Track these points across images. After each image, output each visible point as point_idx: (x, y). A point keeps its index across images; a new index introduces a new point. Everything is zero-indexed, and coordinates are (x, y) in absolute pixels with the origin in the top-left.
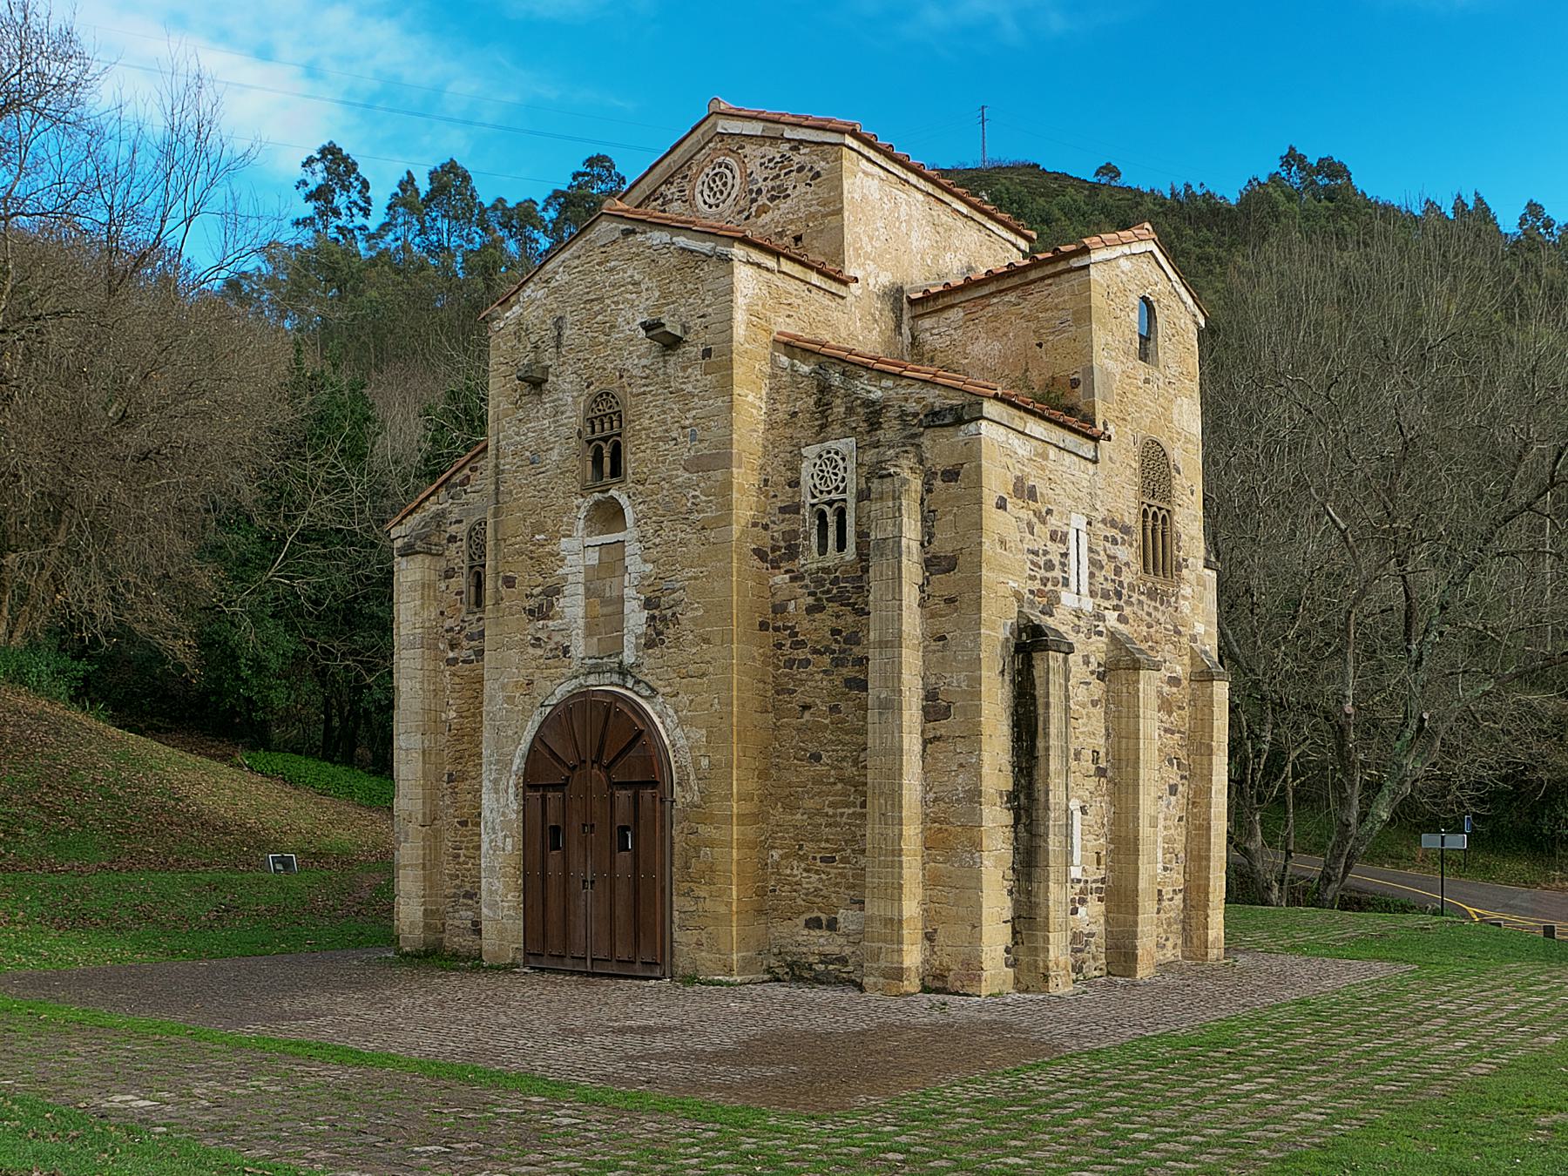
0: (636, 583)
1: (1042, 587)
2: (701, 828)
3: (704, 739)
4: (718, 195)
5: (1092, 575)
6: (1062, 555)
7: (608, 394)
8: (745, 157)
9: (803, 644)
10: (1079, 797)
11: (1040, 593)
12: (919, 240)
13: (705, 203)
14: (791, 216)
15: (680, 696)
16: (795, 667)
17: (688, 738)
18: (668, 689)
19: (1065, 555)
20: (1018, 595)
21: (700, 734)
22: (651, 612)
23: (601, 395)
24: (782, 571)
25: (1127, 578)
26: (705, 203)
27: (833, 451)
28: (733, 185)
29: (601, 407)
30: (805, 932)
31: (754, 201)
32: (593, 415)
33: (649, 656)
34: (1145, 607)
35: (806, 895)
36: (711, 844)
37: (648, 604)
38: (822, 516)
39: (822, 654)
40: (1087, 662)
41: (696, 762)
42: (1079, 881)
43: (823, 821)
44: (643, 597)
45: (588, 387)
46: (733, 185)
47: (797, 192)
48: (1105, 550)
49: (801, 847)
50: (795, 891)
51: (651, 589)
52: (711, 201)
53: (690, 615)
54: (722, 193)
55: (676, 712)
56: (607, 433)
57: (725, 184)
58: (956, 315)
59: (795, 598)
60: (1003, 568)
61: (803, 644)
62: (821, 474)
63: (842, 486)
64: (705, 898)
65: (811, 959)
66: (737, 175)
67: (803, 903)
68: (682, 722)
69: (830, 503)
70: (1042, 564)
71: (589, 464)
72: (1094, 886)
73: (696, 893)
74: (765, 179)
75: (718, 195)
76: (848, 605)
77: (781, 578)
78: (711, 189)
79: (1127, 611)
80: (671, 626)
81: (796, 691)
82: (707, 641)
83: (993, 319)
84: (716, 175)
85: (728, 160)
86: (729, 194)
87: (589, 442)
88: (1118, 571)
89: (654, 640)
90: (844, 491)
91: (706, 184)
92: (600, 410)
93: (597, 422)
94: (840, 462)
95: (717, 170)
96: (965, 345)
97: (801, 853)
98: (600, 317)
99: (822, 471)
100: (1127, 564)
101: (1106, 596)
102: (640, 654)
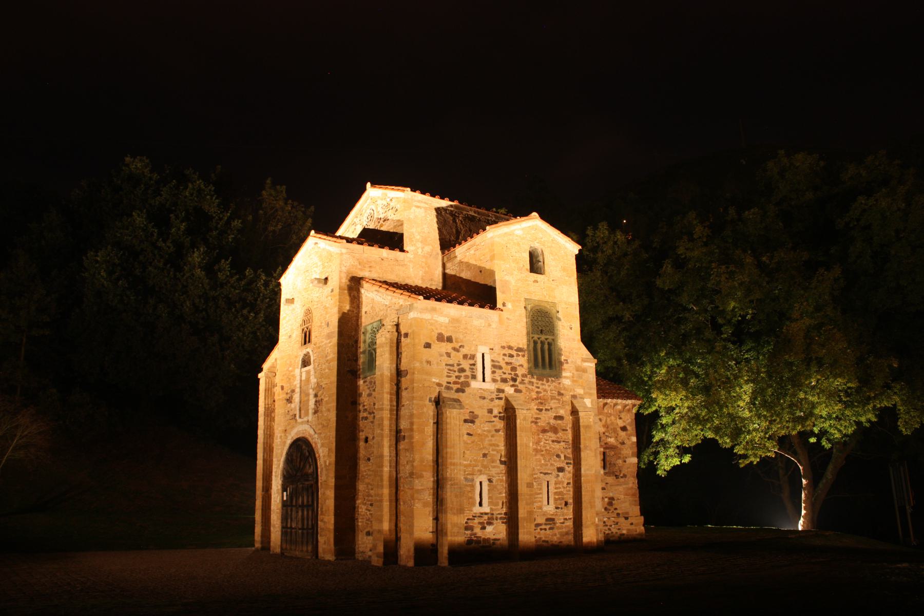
1: (457, 380)
5: (493, 372)
6: (471, 365)
10: (486, 474)
11: (455, 383)
15: (321, 435)
19: (474, 365)
20: (439, 385)
25: (520, 372)
31: (379, 222)
34: (535, 385)
37: (316, 396)
40: (490, 411)
41: (325, 462)
42: (486, 514)
43: (370, 487)
48: (504, 359)
53: (325, 400)
60: (429, 374)
70: (456, 369)
72: (499, 516)
79: (521, 387)
88: (514, 369)
100: (521, 366)
101: (504, 381)
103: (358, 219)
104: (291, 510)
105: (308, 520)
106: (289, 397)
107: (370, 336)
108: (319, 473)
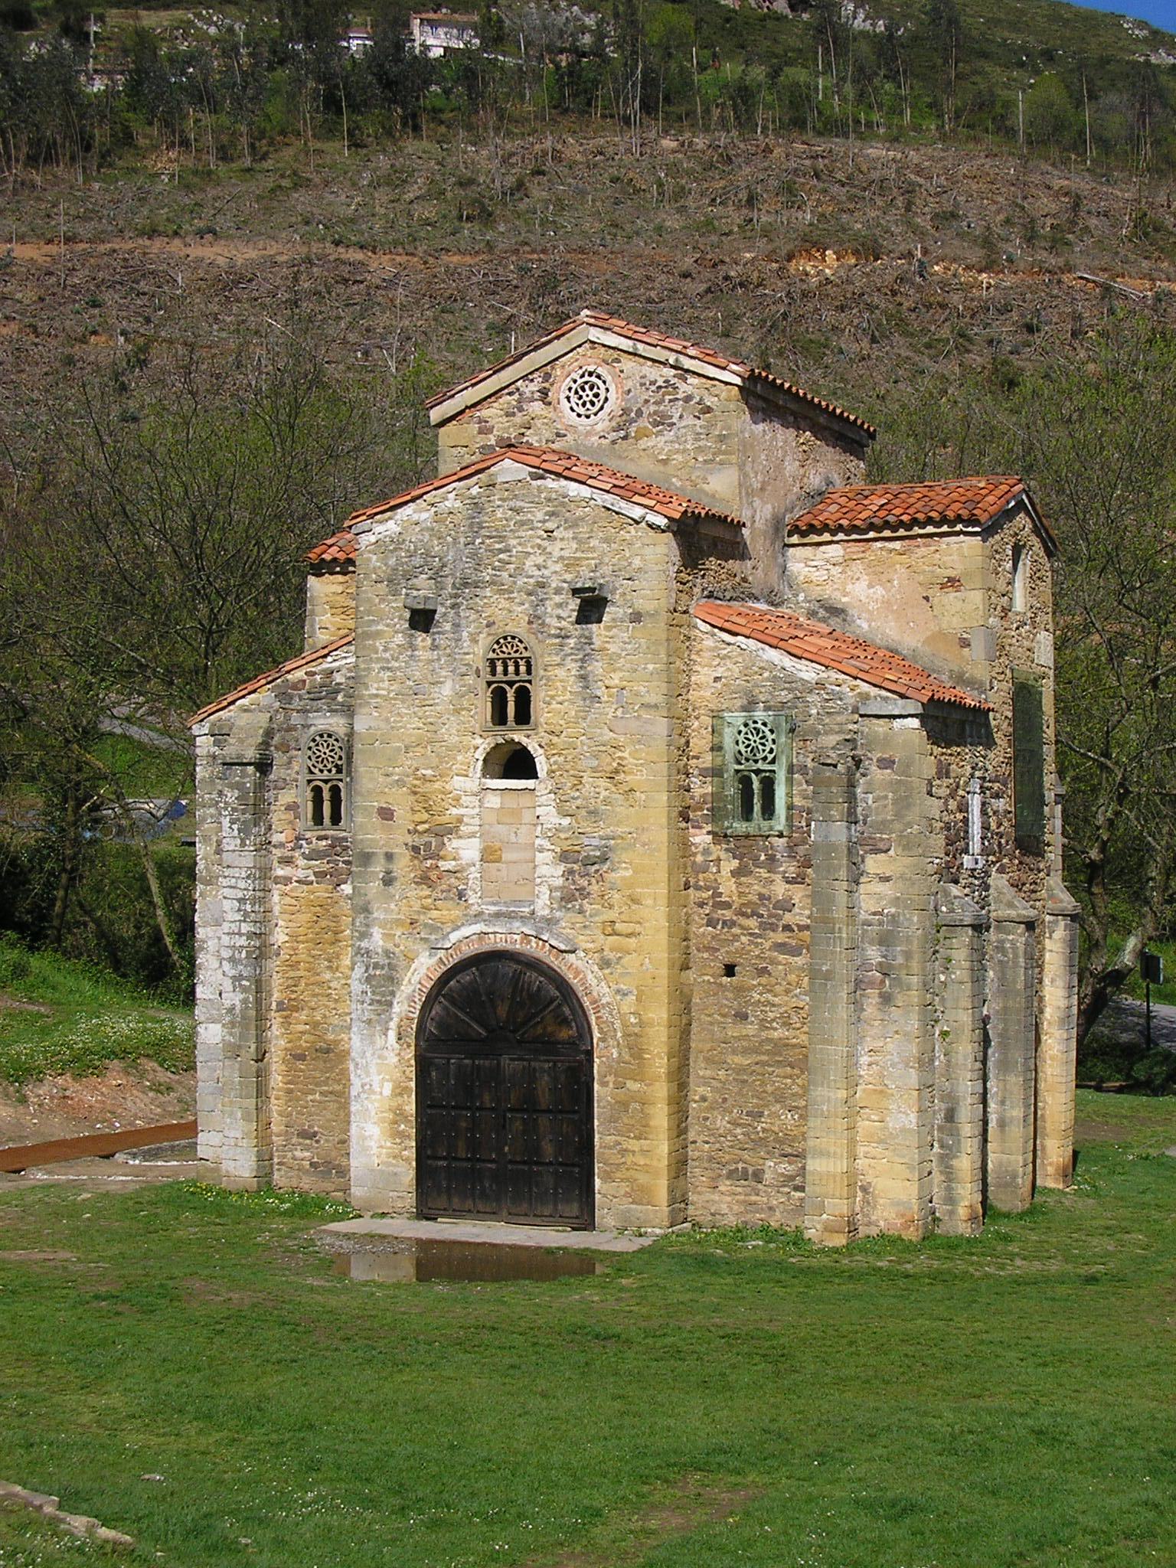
0: (550, 834)
2: (630, 1084)
4: (588, 405)
7: (513, 638)
8: (622, 371)
9: (727, 905)
12: (791, 467)
13: (572, 409)
14: (677, 446)
16: (719, 927)
18: (591, 945)
22: (569, 866)
23: (505, 638)
24: (704, 831)
26: (572, 409)
27: (760, 722)
28: (606, 399)
29: (504, 649)
32: (494, 656)
37: (564, 857)
38: (746, 782)
39: (748, 917)
44: (558, 850)
45: (488, 626)
46: (606, 399)
47: (684, 423)
49: (725, 1100)
51: (569, 842)
52: (582, 410)
54: (593, 404)
56: (511, 677)
57: (596, 395)
58: (835, 551)
61: (727, 905)
62: (747, 742)
63: (770, 757)
64: (634, 1151)
66: (612, 388)
69: (757, 772)
71: (489, 704)
74: (647, 401)
75: (588, 405)
76: (779, 873)
77: (701, 838)
78: (581, 398)
80: (593, 881)
83: (876, 563)
84: (586, 383)
85: (599, 371)
86: (602, 408)
87: (489, 684)
90: (773, 762)
91: (573, 391)
92: (503, 652)
93: (499, 664)
94: (768, 733)
95: (587, 378)
96: (844, 584)
98: (501, 556)
99: (749, 740)
103: (534, 387)
106: (428, 845)
107: (741, 738)
108: (595, 1041)
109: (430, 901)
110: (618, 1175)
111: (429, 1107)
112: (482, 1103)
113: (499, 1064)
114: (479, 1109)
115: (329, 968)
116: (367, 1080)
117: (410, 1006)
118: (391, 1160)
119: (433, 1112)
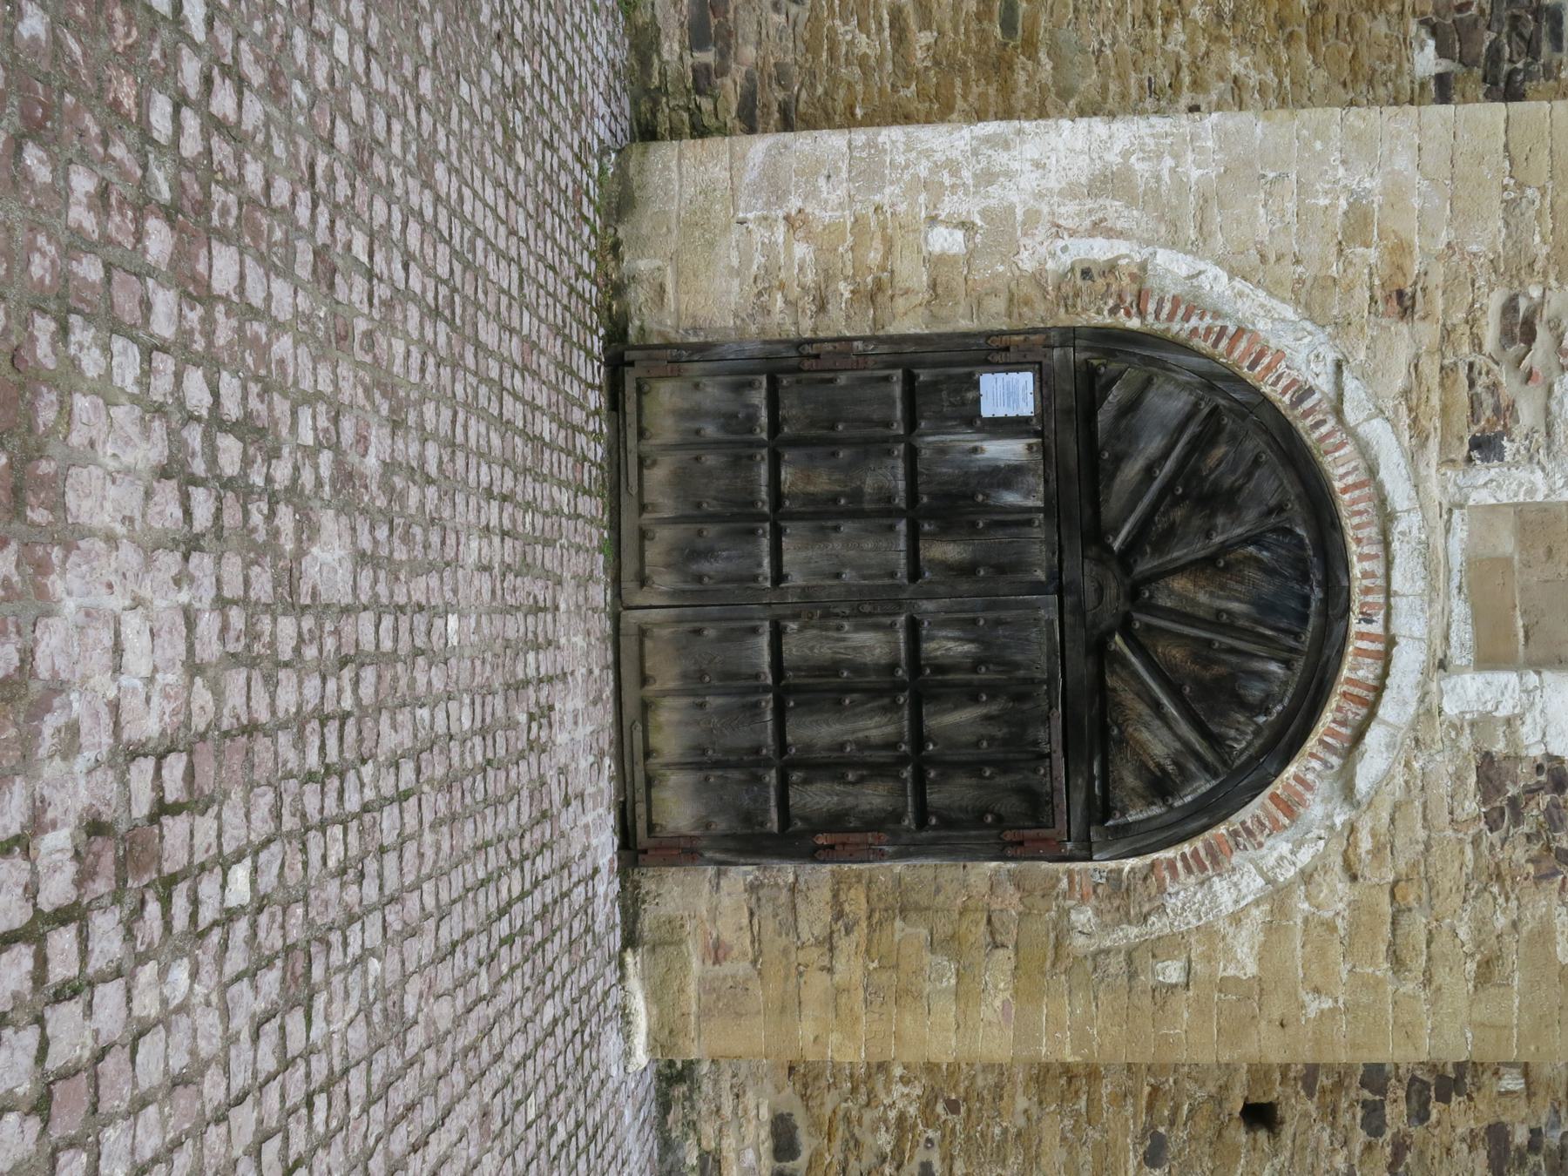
3: (1231, 972)
15: (1343, 887)
16: (1367, 1094)
17: (1236, 919)
18: (1365, 843)
21: (1244, 959)
30: (765, 1114)
33: (1459, 777)
35: (847, 1119)
36: (966, 992)
49: (953, 1107)
50: (854, 1090)
55: (1306, 877)
59: (1530, 1094)
61: (1421, 1115)
64: (830, 970)
65: (708, 1129)
67: (827, 1112)
68: (1277, 896)
73: (845, 944)
81: (1310, 1095)
82: (1487, 971)
89: (1500, 790)
97: (940, 1108)
102: (1466, 742)
104: (881, 513)
105: (831, 766)
109: (1466, 349)
110: (770, 926)
111: (909, 379)
112: (933, 536)
113: (1037, 588)
114: (914, 536)
115: (1219, 16)
116: (966, 174)
117: (1176, 301)
118: (759, 259)
119: (897, 390)
